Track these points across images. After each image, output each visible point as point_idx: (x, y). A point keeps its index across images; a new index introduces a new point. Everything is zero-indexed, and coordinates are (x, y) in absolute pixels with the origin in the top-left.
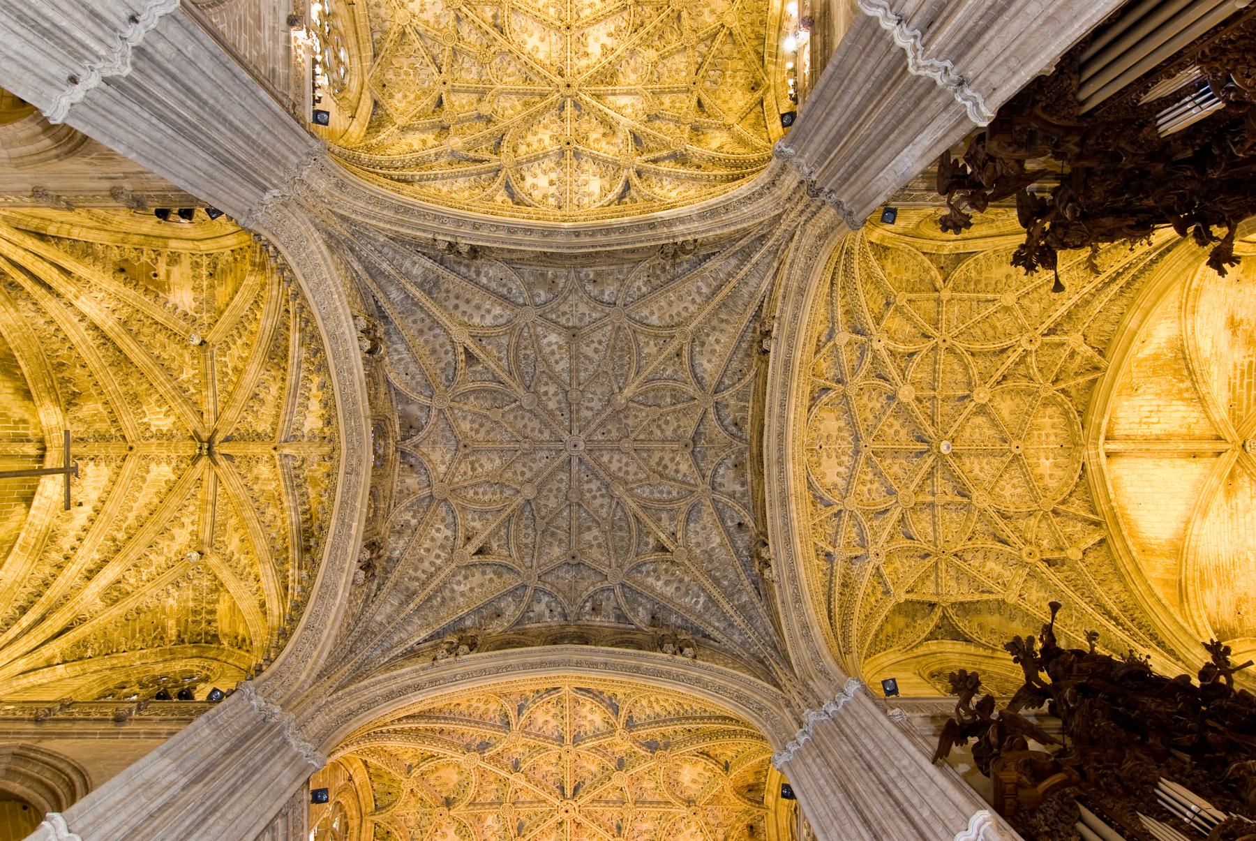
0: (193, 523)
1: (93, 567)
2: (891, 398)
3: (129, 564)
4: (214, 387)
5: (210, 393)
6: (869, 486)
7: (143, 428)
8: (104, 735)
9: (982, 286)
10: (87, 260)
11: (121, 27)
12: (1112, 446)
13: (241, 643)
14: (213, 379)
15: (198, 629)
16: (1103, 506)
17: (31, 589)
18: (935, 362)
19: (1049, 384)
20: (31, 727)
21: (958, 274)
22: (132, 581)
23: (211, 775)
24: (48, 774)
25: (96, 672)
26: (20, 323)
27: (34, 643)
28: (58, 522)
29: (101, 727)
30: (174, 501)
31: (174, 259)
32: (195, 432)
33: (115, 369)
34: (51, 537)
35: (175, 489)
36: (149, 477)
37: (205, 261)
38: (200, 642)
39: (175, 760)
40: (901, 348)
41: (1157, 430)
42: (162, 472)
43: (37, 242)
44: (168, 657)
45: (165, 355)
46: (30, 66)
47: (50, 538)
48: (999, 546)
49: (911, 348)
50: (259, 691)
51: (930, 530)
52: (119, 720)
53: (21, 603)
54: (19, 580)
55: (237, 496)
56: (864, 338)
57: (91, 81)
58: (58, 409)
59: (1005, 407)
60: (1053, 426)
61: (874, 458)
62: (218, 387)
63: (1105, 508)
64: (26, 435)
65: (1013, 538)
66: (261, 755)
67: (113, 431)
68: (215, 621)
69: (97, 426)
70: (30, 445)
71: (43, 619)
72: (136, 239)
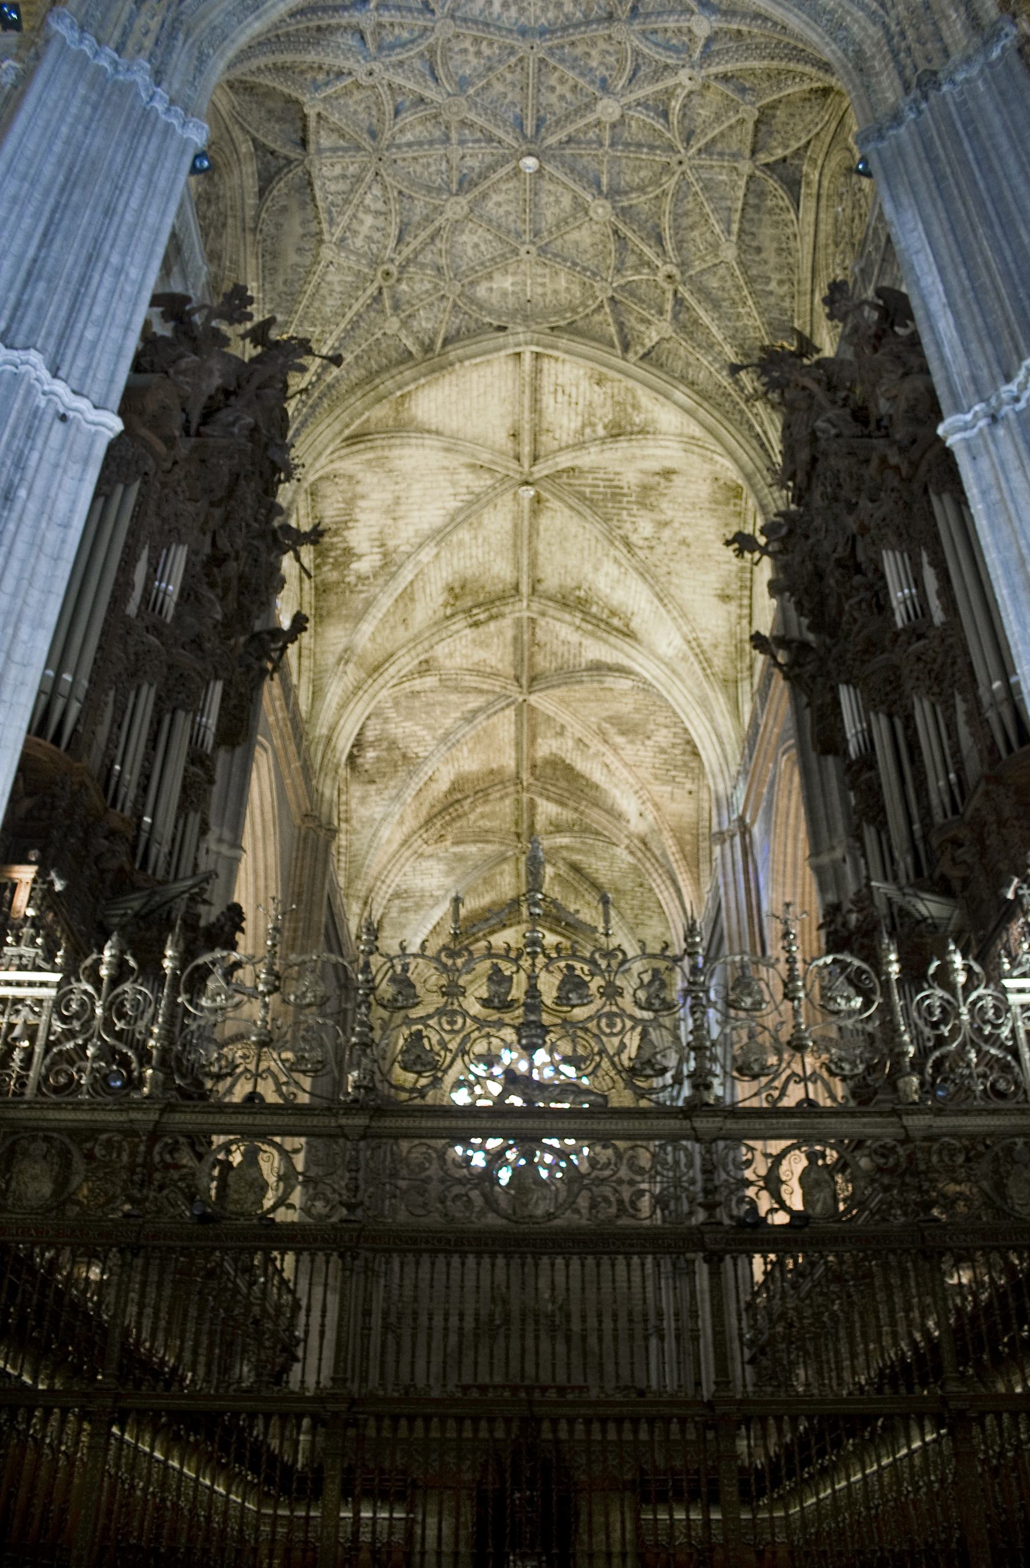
2: (604, 85)
6: (472, 49)
9: (751, 213)
12: (527, 358)
16: (454, 352)
18: (652, 148)
19: (610, 293)
21: (772, 184)
40: (676, 105)
41: (548, 400)
48: (394, 231)
49: (674, 119)
51: (409, 137)
56: (696, 55)
59: (583, 236)
60: (556, 292)
61: (513, 60)
63: (452, 356)
65: (407, 251)
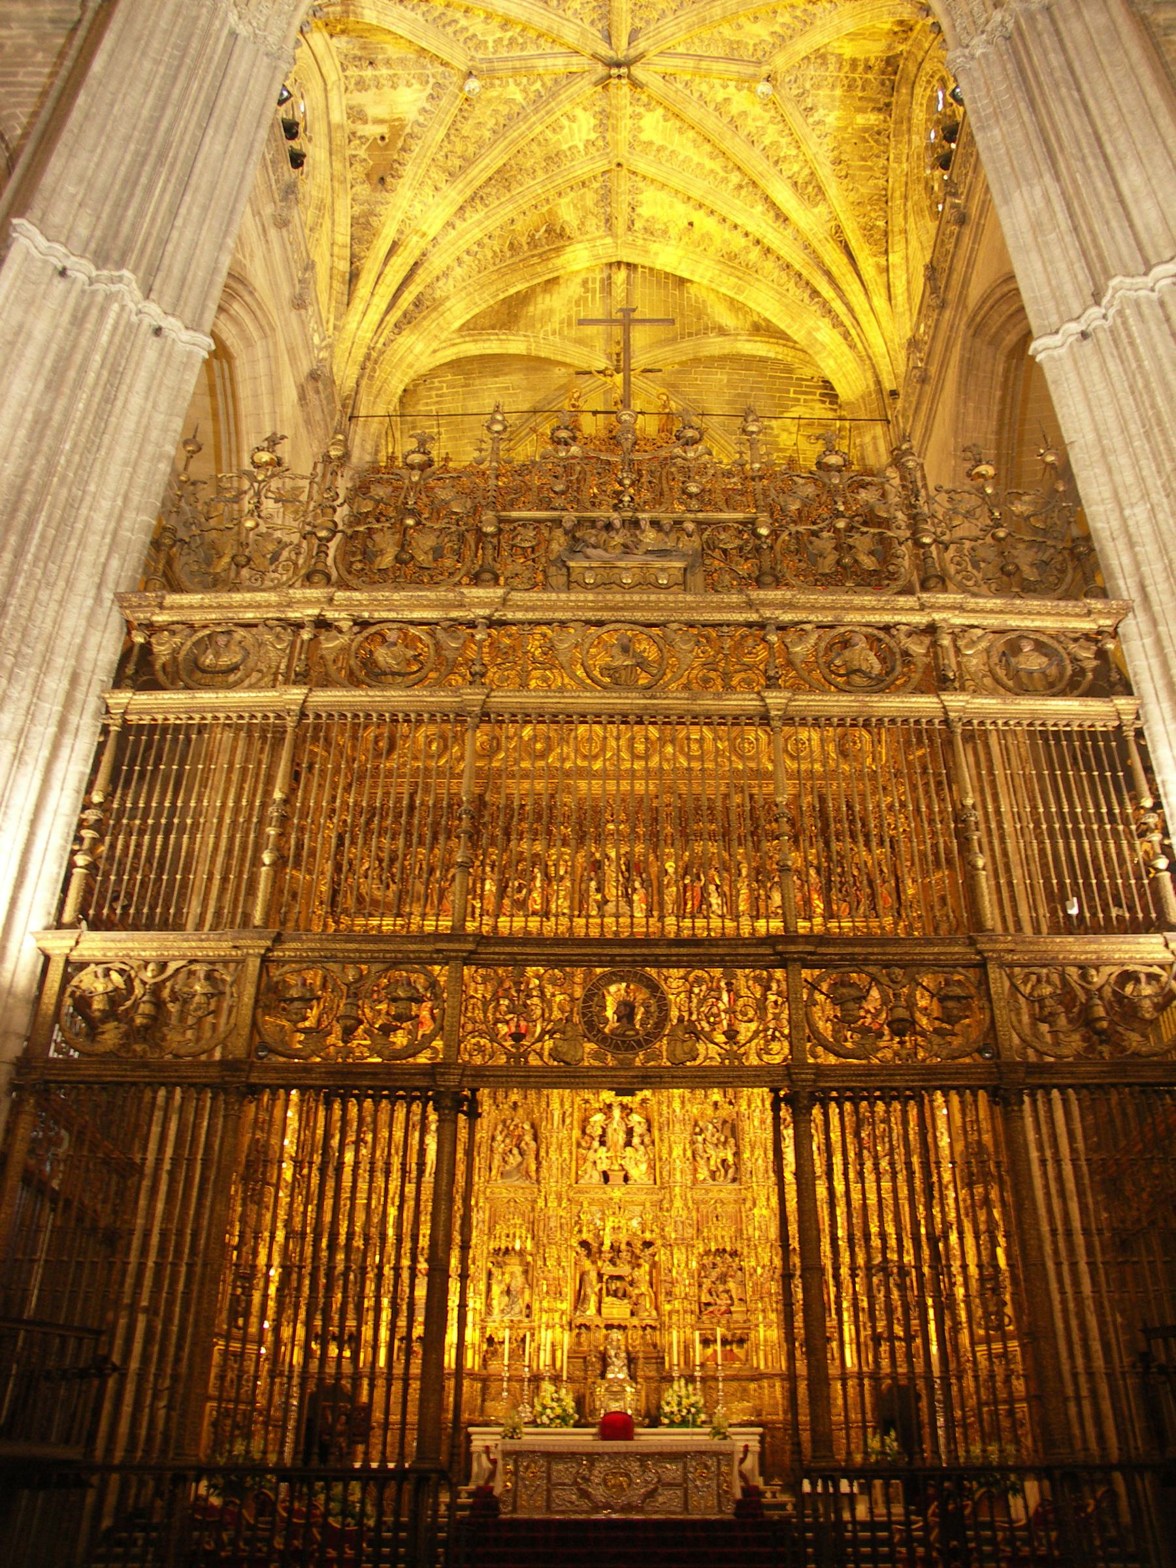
0: (725, 87)
1: (772, 214)
3: (774, 171)
4: (531, 57)
5: (541, 63)
7: (592, 150)
8: (976, 239)
10: (375, 224)
11: (77, 287)
13: (905, 28)
14: (520, 58)
15: (875, 84)
17: (792, 284)
20: (948, 314)
22: (796, 168)
23: (1052, 138)
24: (1004, 307)
25: (905, 218)
26: (463, 294)
27: (857, 286)
28: (712, 249)
29: (966, 240)
30: (693, 112)
31: (357, 114)
32: (596, 84)
33: (514, 184)
34: (730, 259)
35: (677, 111)
36: (659, 141)
37: (352, 72)
38: (893, 82)
39: (1019, 186)
42: (653, 125)
43: (361, 283)
44: (905, 127)
45: (491, 123)
46: (156, 382)
47: (730, 259)
50: (965, 42)
52: (962, 220)
53: (806, 296)
54: (777, 297)
55: (690, 27)
57: (154, 312)
58: (569, 249)
62: (531, 50)
64: (602, 280)
66: (1052, 56)
67: (596, 185)
68: (867, 60)
69: (589, 203)
70: (614, 277)
71: (828, 274)
72: (338, 166)
